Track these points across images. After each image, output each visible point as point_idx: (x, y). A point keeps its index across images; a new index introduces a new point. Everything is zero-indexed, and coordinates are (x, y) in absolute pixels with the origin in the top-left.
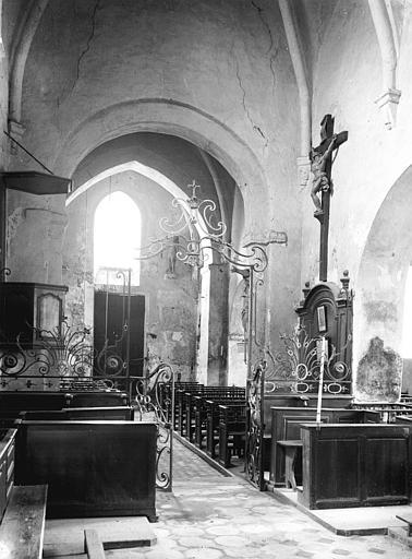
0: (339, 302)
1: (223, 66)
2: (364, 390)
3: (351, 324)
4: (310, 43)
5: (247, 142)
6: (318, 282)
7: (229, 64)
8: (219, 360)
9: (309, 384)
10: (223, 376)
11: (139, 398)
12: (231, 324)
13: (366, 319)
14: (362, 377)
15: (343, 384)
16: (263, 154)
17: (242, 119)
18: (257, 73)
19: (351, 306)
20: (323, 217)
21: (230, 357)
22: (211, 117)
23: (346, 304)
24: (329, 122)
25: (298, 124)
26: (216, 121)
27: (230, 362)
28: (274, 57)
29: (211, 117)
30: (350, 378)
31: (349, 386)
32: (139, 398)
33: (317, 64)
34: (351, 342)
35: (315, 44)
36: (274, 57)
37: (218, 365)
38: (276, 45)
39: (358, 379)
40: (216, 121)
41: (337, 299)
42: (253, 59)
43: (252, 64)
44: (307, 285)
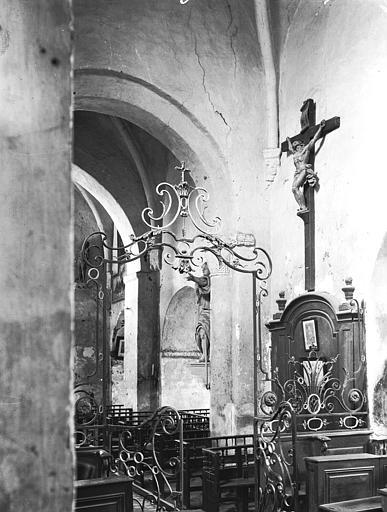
0: (340, 316)
1: (180, 40)
2: (381, 421)
3: (363, 344)
4: (279, 22)
5: (208, 129)
6: (300, 290)
7: (187, 38)
8: (149, 380)
9: (323, 418)
10: (155, 399)
11: (125, 457)
12: (162, 338)
13: (379, 335)
14: (378, 406)
15: (358, 416)
16: (226, 142)
17: (203, 102)
18: (216, 51)
19: (363, 321)
20: (308, 218)
21: (162, 377)
22: (167, 97)
23: (357, 317)
24: (310, 107)
25: (263, 110)
26: (174, 102)
27: (163, 383)
28: (234, 35)
29: (167, 97)
30: (365, 408)
31: (365, 418)
32: (125, 457)
33: (285, 46)
34: (365, 364)
35: (283, 23)
36: (234, 35)
37: (149, 386)
38: (236, 22)
39: (375, 408)
40: (174, 102)
41: (338, 312)
42: (212, 36)
43: (211, 40)
44: (282, 295)
